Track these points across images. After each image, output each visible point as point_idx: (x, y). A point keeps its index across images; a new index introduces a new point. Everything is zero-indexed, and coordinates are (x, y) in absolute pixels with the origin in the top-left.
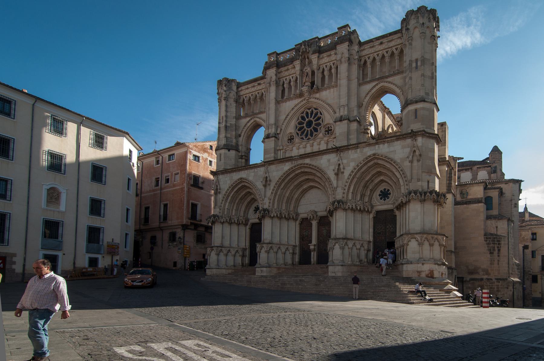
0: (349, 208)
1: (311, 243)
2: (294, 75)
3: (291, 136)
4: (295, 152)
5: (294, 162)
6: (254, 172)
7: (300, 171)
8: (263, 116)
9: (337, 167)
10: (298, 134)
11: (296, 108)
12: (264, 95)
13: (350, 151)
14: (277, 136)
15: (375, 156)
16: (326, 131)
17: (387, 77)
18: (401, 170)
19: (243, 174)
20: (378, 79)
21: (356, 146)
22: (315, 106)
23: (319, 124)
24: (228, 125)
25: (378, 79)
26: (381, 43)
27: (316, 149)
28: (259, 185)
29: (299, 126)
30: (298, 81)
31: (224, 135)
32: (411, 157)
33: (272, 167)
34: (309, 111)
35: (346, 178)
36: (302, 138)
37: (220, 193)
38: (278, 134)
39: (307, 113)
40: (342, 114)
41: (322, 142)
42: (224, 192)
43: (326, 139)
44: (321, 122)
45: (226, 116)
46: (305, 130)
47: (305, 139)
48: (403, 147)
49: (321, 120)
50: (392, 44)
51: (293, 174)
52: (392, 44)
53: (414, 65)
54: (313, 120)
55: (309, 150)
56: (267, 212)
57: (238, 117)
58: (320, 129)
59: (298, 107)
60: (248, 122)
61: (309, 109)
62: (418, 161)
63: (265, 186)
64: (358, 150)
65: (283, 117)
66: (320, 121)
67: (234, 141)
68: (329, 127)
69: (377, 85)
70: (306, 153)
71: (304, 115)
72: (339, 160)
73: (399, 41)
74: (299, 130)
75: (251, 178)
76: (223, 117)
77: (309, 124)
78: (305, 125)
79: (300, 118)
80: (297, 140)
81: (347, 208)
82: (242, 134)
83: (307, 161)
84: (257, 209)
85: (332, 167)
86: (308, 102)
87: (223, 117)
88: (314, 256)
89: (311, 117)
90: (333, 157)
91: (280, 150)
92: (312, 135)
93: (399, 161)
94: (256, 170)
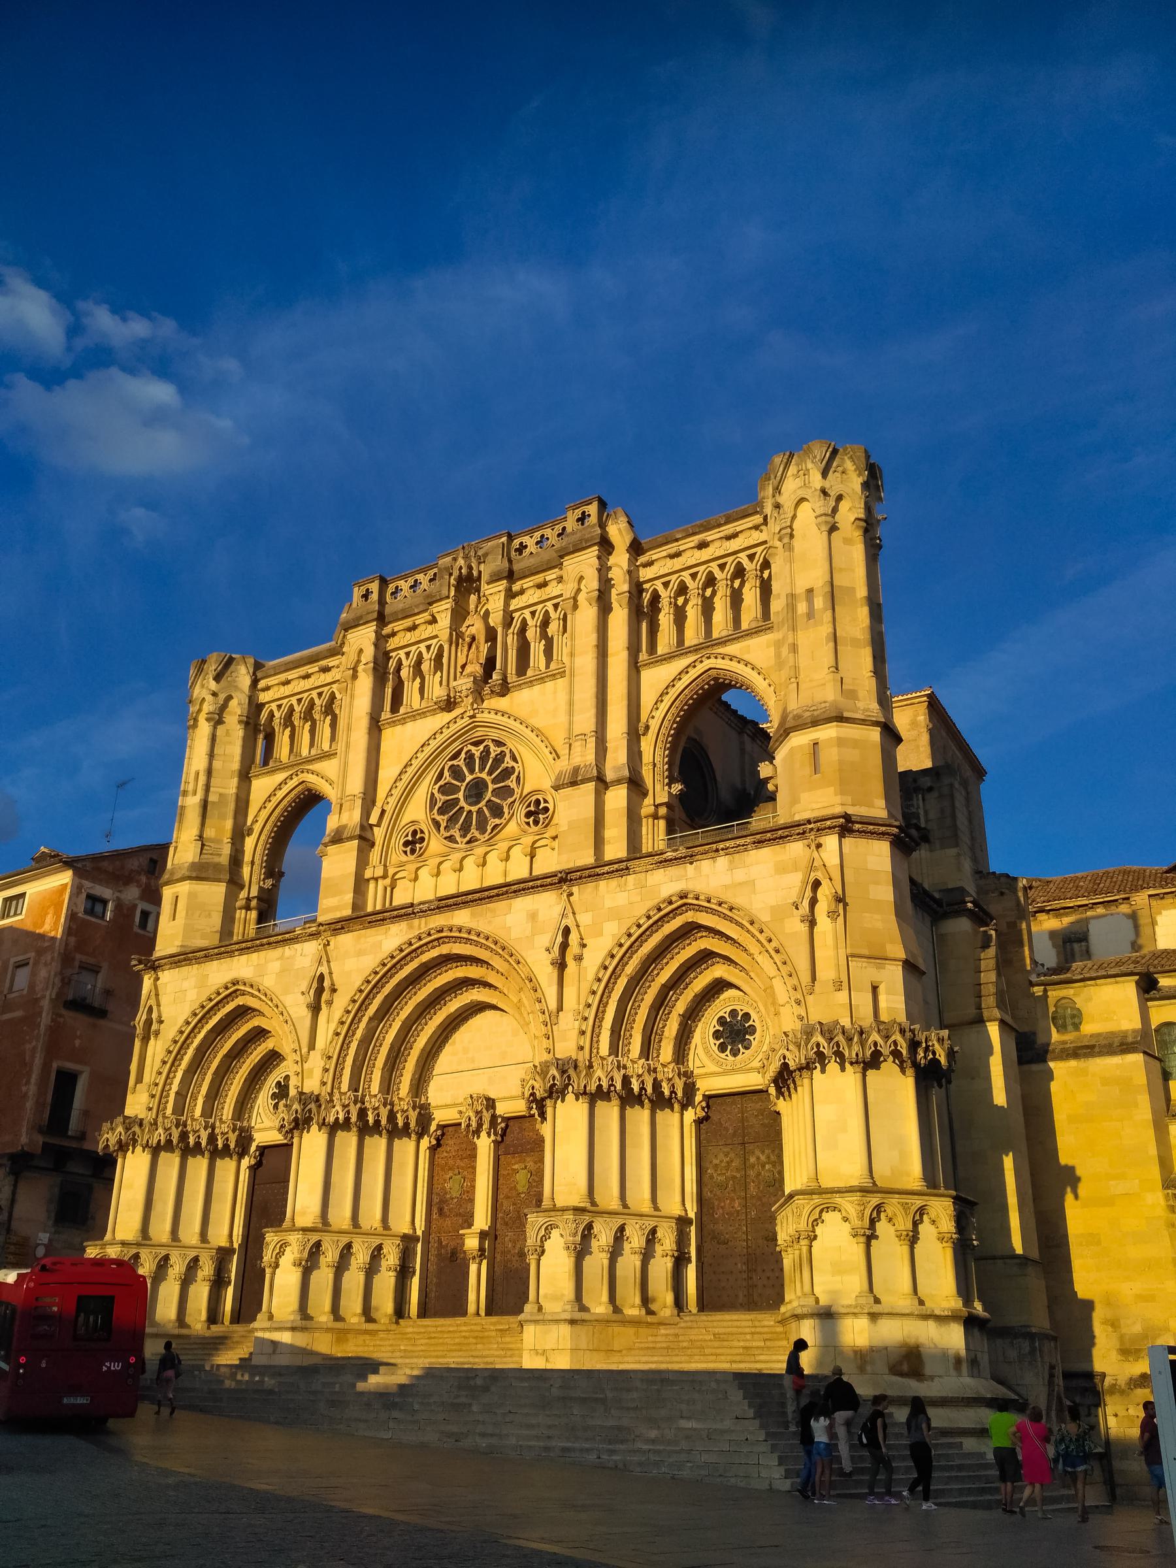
0: (600, 1087)
1: (470, 1225)
2: (434, 641)
3: (415, 833)
4: (425, 889)
5: (416, 922)
6: (281, 958)
7: (434, 953)
8: (329, 767)
9: (560, 939)
10: (437, 824)
11: (434, 744)
12: (337, 703)
13: (602, 884)
14: (368, 835)
15: (683, 901)
16: (529, 814)
17: (724, 642)
18: (777, 951)
19: (242, 967)
21: (620, 868)
22: (495, 734)
23: (507, 792)
24: (212, 798)
25: (696, 649)
26: (703, 545)
27: (494, 875)
29: (441, 798)
30: (445, 660)
31: (195, 832)
32: (806, 903)
33: (344, 941)
34: (477, 751)
35: (591, 976)
36: (451, 839)
37: (157, 1033)
38: (371, 826)
39: (470, 757)
41: (516, 852)
43: (528, 840)
44: (513, 785)
45: (209, 772)
47: (462, 842)
48: (781, 869)
49: (514, 777)
50: (734, 545)
51: (414, 965)
52: (734, 545)
53: (802, 607)
54: (488, 779)
55: (471, 880)
56: (313, 1106)
57: (245, 777)
60: (279, 787)
61: (477, 744)
62: (833, 915)
63: (315, 1009)
65: (387, 773)
66: (511, 783)
67: (226, 850)
68: (538, 802)
69: (693, 665)
70: (463, 889)
71: (460, 762)
73: (757, 537)
74: (441, 811)
75: (268, 982)
76: (197, 774)
77: (476, 790)
78: (461, 795)
80: (435, 844)
81: (592, 1088)
82: (257, 828)
83: (461, 917)
84: (282, 1090)
85: (545, 940)
87: (197, 774)
88: (477, 1277)
89: (482, 770)
90: (548, 904)
91: (376, 879)
92: (482, 828)
93: (764, 917)
94: (288, 951)
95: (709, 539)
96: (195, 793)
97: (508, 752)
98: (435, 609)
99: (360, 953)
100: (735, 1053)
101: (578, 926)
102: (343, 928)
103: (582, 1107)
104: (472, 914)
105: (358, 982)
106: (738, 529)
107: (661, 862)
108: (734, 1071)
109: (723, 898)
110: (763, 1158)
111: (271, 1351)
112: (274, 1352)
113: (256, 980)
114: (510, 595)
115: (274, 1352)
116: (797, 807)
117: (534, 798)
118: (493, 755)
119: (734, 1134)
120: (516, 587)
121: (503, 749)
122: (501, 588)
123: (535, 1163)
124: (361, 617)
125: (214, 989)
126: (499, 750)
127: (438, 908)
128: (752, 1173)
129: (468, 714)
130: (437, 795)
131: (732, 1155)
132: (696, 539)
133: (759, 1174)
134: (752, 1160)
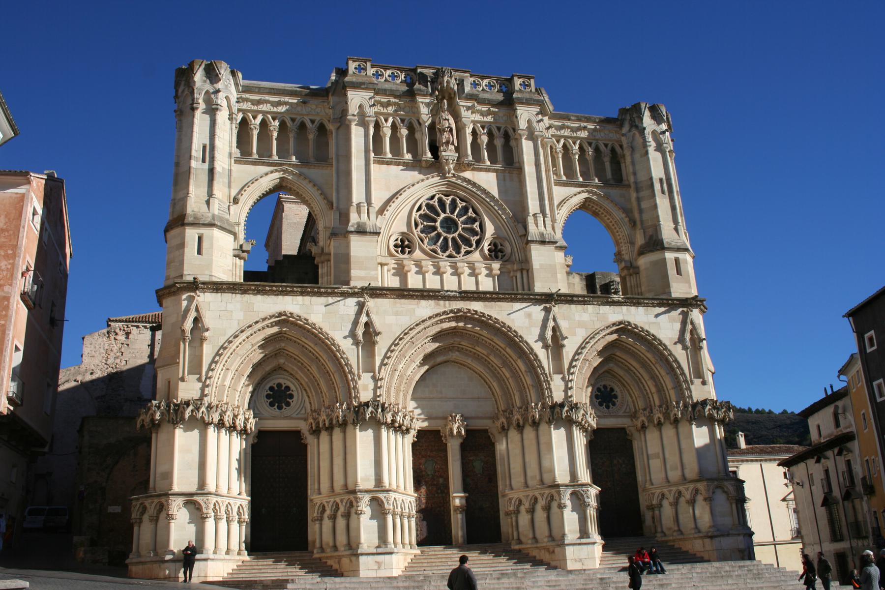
3: (402, 241)
5: (442, 302)
7: (453, 324)
10: (422, 241)
13: (573, 306)
20: (581, 186)
34: (448, 201)
46: (439, 235)
64: (590, 307)
66: (476, 226)
72: (554, 320)
77: (450, 225)
78: (438, 224)
79: (424, 207)
83: (477, 306)
87: (204, 147)
89: (452, 212)
90: (537, 312)
99: (397, 314)
100: (608, 407)
103: (656, 434)
108: (611, 416)
109: (646, 328)
111: (376, 567)
112: (379, 568)
113: (304, 316)
116: (672, 290)
124: (364, 84)
130: (419, 221)
134: (615, 462)
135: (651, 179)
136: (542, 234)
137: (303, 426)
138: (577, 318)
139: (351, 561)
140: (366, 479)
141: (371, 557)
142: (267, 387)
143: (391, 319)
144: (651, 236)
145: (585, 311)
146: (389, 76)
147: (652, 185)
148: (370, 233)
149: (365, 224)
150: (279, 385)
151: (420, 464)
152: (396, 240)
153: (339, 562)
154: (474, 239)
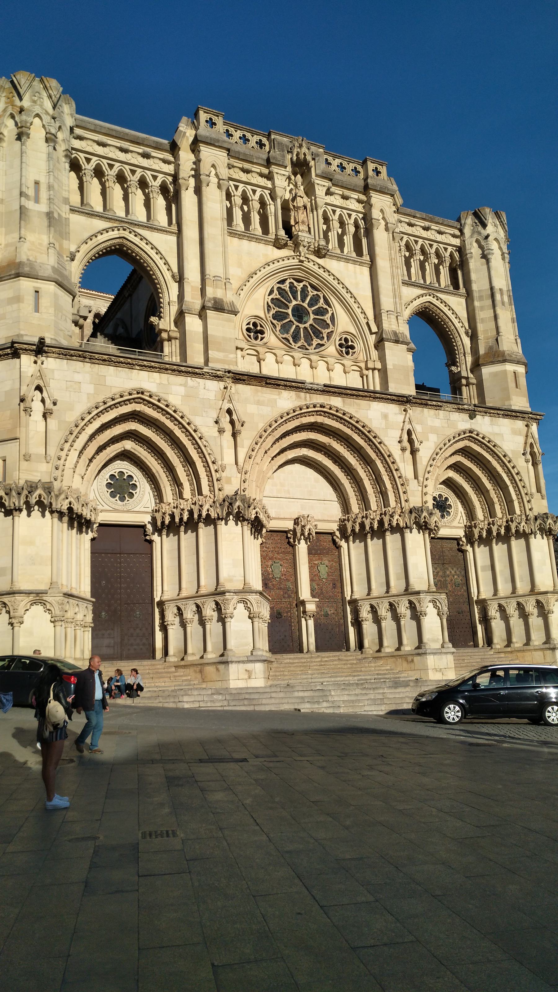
3: (255, 324)
5: (302, 394)
6: (185, 385)
11: (272, 267)
13: (426, 410)
22: (315, 281)
28: (204, 424)
34: (299, 286)
39: (292, 286)
40: (394, 327)
42: (72, 416)
50: (439, 238)
52: (439, 238)
58: (329, 335)
59: (277, 265)
61: (299, 281)
64: (441, 412)
66: (327, 318)
73: (457, 242)
77: (300, 314)
78: (290, 311)
79: (276, 291)
83: (336, 402)
85: (397, 434)
86: (300, 266)
87: (37, 183)
89: (303, 302)
93: (510, 454)
95: (432, 227)
96: (37, 200)
97: (322, 296)
98: (274, 169)
99: (259, 403)
101: (402, 430)
102: (244, 380)
104: (344, 402)
105: (261, 425)
106: (447, 231)
107: (462, 409)
109: (492, 438)
110: (453, 572)
111: (246, 677)
113: (162, 395)
114: (328, 193)
115: (249, 678)
117: (344, 336)
118: (311, 294)
119: (439, 559)
120: (333, 189)
121: (319, 293)
122: (326, 184)
123: (329, 561)
125: (115, 391)
126: (315, 293)
127: (324, 391)
128: (448, 579)
129: (301, 258)
130: (270, 304)
131: (438, 569)
132: (427, 224)
133: (452, 580)
134: (448, 572)
135: (492, 288)
136: (395, 333)
137: (146, 519)
138: (430, 423)
139: (217, 670)
140: (230, 580)
141: (241, 665)
142: (108, 476)
143: (252, 409)
144: (491, 348)
145: (437, 417)
146: (240, 138)
147: (493, 296)
148: (229, 311)
149: (222, 300)
150: (121, 473)
151: (267, 566)
152: (248, 324)
153: (201, 672)
154: (325, 332)
